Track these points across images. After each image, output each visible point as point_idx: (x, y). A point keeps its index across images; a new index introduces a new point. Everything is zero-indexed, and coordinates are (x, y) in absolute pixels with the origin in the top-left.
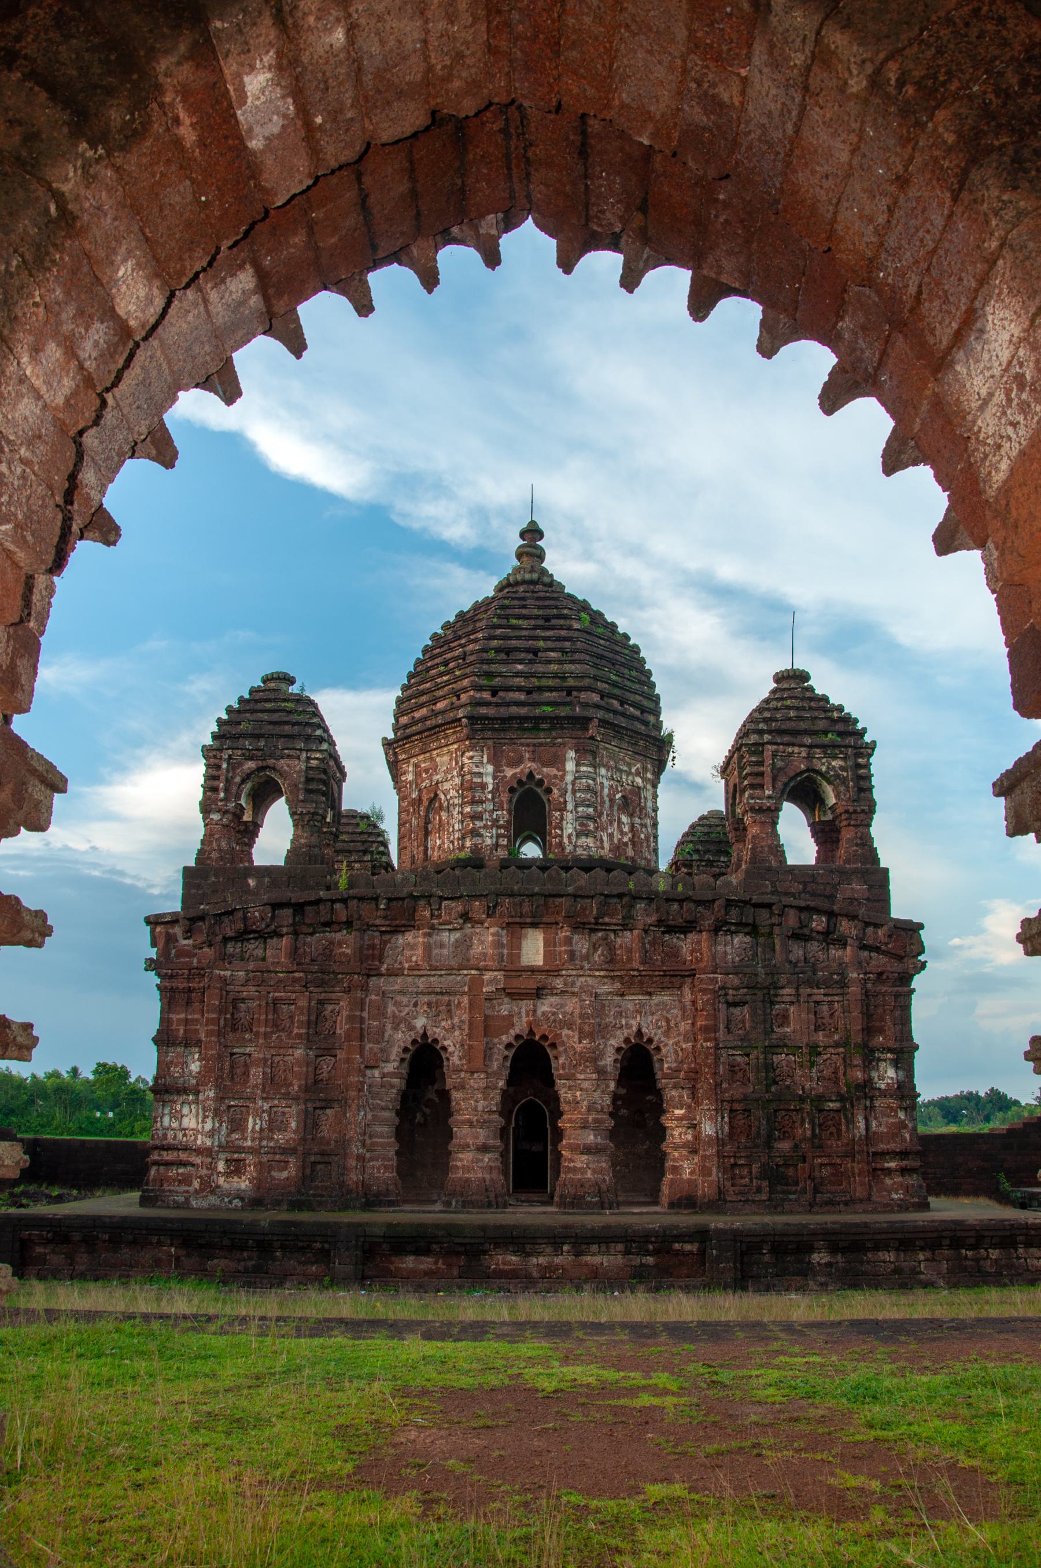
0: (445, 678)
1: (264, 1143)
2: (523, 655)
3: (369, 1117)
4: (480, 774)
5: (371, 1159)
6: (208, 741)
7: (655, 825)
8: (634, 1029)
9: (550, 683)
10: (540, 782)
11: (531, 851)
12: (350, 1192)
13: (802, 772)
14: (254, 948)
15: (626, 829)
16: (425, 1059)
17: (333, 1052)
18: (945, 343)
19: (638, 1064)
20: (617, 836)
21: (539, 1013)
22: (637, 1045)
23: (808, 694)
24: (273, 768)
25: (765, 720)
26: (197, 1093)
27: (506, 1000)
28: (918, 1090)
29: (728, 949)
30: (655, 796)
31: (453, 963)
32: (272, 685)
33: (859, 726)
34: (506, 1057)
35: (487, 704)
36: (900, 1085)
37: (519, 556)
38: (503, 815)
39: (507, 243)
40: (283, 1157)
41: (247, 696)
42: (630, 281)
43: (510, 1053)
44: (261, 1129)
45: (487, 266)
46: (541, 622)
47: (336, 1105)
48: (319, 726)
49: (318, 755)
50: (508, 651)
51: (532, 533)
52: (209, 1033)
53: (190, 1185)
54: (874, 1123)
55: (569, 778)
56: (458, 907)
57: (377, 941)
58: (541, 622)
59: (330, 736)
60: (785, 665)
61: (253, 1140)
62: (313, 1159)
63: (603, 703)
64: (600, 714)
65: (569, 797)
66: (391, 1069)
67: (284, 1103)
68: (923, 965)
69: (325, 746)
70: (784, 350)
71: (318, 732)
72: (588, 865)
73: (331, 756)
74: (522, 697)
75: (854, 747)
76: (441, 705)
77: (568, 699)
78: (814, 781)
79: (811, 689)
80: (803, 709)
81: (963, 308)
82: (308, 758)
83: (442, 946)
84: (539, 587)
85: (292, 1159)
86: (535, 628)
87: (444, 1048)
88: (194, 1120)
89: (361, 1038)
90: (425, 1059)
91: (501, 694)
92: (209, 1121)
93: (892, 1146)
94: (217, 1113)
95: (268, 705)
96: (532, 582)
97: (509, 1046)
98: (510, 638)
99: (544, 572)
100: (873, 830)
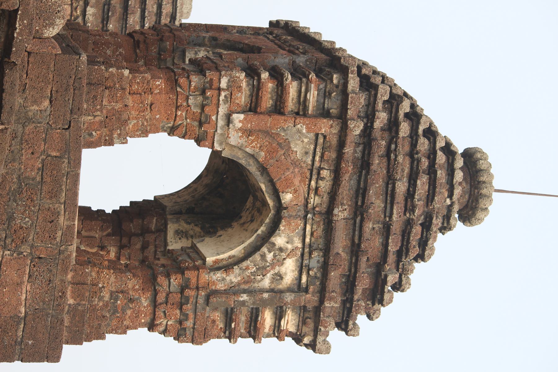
23: (437, 222)
25: (393, 126)
33: (361, 319)
75: (318, 310)
79: (445, 228)
80: (409, 207)
100: (140, 335)
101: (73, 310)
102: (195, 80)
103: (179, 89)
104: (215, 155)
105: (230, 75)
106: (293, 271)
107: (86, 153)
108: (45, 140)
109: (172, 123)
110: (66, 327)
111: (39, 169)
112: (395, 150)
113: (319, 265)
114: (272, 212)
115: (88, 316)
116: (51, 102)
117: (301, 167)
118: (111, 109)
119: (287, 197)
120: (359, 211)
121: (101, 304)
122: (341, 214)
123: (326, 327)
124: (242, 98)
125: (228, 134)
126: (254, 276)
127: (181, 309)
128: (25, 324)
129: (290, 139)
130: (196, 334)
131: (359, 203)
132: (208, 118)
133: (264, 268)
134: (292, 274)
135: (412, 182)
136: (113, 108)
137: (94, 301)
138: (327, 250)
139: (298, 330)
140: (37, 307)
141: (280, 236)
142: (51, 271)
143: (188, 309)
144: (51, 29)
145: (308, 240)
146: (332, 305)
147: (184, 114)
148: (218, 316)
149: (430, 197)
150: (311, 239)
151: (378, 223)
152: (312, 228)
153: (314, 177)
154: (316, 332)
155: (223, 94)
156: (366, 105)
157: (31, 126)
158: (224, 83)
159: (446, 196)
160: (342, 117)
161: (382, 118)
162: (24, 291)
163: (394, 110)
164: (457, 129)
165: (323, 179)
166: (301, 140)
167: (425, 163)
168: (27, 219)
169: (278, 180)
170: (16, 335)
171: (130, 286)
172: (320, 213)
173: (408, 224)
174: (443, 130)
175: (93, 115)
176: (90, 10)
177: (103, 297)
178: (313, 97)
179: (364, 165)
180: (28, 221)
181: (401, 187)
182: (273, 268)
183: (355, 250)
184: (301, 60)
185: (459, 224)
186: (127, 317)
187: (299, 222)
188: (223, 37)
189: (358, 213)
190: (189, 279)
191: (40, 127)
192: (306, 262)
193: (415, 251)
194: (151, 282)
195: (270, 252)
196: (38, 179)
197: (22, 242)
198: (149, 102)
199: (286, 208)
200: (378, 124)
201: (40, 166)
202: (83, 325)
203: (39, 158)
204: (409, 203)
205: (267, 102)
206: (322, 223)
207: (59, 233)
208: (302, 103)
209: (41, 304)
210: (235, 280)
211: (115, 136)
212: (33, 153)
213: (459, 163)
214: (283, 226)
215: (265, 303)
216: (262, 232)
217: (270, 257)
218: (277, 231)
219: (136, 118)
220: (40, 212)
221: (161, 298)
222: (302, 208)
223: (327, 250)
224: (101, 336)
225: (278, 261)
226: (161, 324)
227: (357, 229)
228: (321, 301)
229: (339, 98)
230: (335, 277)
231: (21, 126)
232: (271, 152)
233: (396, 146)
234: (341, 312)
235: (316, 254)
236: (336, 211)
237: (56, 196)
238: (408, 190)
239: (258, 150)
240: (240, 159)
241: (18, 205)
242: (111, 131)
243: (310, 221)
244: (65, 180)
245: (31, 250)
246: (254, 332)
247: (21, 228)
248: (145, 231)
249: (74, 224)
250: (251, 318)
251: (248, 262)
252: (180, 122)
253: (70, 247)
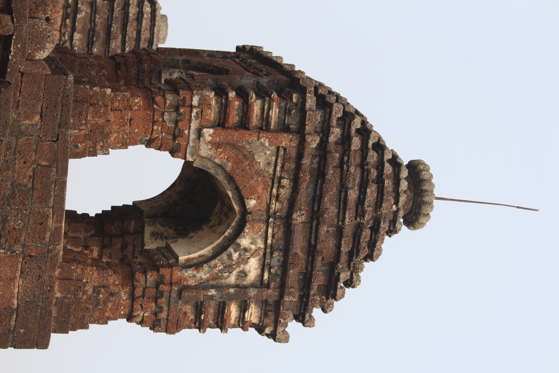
13: (242, 201)
23: (385, 226)
25: (346, 140)
33: (317, 312)
75: (278, 303)
78: (223, 222)
79: (392, 231)
80: (360, 212)
100: (120, 326)
101: (60, 303)
102: (170, 98)
103: (155, 106)
104: (187, 166)
105: (201, 94)
106: (256, 269)
107: (73, 163)
108: (36, 151)
109: (149, 136)
110: (54, 317)
111: (30, 177)
112: (348, 162)
113: (280, 264)
114: (238, 216)
115: (73, 308)
116: (41, 117)
117: (264, 176)
118: (94, 124)
119: (252, 203)
120: (315, 216)
121: (85, 297)
122: (299, 218)
123: (285, 319)
124: (212, 114)
125: (199, 147)
126: (222, 273)
127: (156, 302)
128: (17, 315)
129: (254, 151)
130: (169, 325)
131: (316, 209)
132: (181, 132)
133: (231, 266)
134: (255, 271)
135: (363, 190)
136: (97, 123)
137: (79, 294)
138: (286, 250)
139: (260, 321)
140: (28, 300)
141: (245, 238)
142: (40, 268)
143: (163, 301)
144: (42, 52)
145: (269, 241)
146: (291, 299)
147: (160, 128)
148: (189, 309)
149: (378, 204)
150: (272, 241)
151: (332, 226)
152: (273, 231)
153: (276, 185)
154: (276, 323)
155: (195, 111)
156: (322, 122)
157: (24, 139)
158: (195, 101)
159: (393, 203)
160: (301, 133)
161: (336, 133)
162: (17, 285)
163: (347, 126)
165: (283, 187)
166: (264, 152)
167: (374, 173)
168: (19, 221)
169: (244, 188)
170: (10, 325)
171: (111, 281)
172: (280, 217)
173: (359, 228)
174: (390, 144)
175: (79, 129)
176: (77, 36)
177: (87, 291)
178: (274, 113)
179: (320, 175)
180: (21, 223)
181: (353, 195)
182: (238, 266)
183: (312, 250)
184: (264, 81)
185: (404, 228)
186: (108, 309)
187: (262, 225)
188: (195, 60)
189: (314, 217)
190: (163, 275)
191: (32, 139)
192: (267, 261)
193: (365, 252)
194: (129, 279)
195: (236, 252)
196: (30, 185)
197: (15, 242)
198: (129, 117)
199: (250, 213)
200: (332, 139)
201: (31, 174)
202: (69, 316)
203: (30, 167)
204: (360, 209)
205: (234, 118)
206: (282, 227)
207: (48, 234)
208: (265, 119)
209: (32, 297)
210: (204, 277)
211: (98, 147)
212: (25, 163)
213: (405, 173)
214: (247, 229)
215: (231, 298)
216: (229, 234)
217: (235, 256)
218: (242, 233)
219: (117, 132)
220: (31, 215)
221: (138, 292)
222: (265, 213)
223: (286, 250)
224: (86, 327)
225: (243, 260)
226: (138, 315)
227: (313, 231)
228: (281, 296)
229: (298, 115)
230: (293, 273)
231: (14, 138)
232: (237, 163)
233: (349, 158)
234: (299, 305)
235: (277, 254)
236: (295, 216)
237: (45, 201)
238: (359, 197)
239: (225, 161)
240: (209, 168)
241: (11, 208)
242: (95, 144)
243: (272, 224)
244: (53, 186)
245: (23, 249)
246: (221, 323)
247: (14, 229)
249: (62, 226)
250: (218, 310)
251: (217, 261)
252: (156, 136)
253: (57, 247)
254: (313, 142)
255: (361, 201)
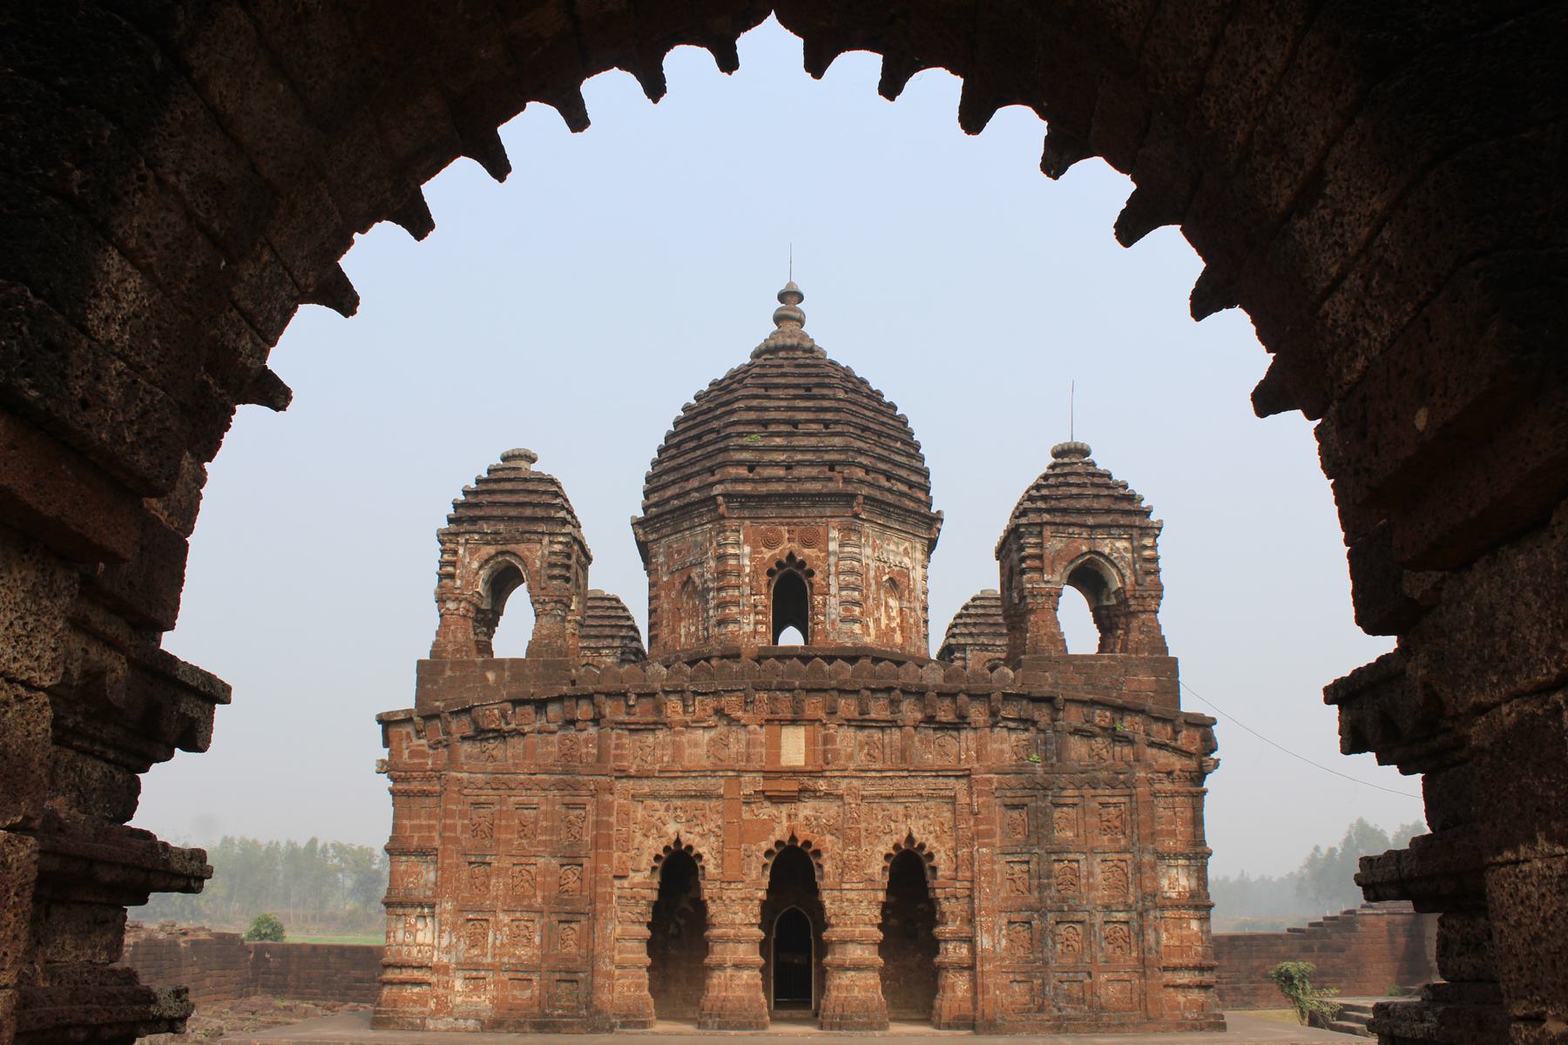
0: (698, 453)
1: (506, 960)
2: (783, 428)
3: (619, 930)
4: (736, 556)
5: (621, 977)
6: (445, 525)
7: (925, 609)
8: (905, 835)
9: (809, 457)
10: (803, 563)
11: (791, 637)
12: (599, 1012)
13: (1083, 554)
14: (493, 746)
15: (894, 614)
16: (679, 868)
17: (578, 861)
18: (1282, 205)
19: (909, 868)
20: (884, 621)
21: (801, 816)
22: (907, 851)
23: (1091, 469)
24: (514, 554)
25: (1043, 498)
26: (432, 906)
27: (767, 804)
28: (1212, 899)
29: (1006, 747)
30: (925, 578)
31: (706, 763)
32: (513, 464)
33: (1144, 504)
34: (765, 866)
35: (744, 480)
36: (1193, 895)
37: (778, 319)
38: (764, 600)
39: (746, 43)
40: (525, 975)
41: (485, 475)
42: (891, 87)
43: (770, 861)
44: (503, 945)
45: (723, 70)
46: (802, 392)
47: (582, 918)
48: (563, 508)
49: (561, 539)
50: (765, 423)
51: (790, 296)
52: (444, 840)
53: (425, 1004)
54: (1164, 936)
55: (832, 560)
56: (711, 702)
57: (626, 741)
58: (802, 392)
59: (574, 517)
60: (1063, 439)
61: (494, 956)
62: (558, 976)
63: (869, 478)
64: (865, 491)
65: (832, 580)
66: (643, 880)
67: (526, 916)
68: (1217, 763)
69: (568, 529)
70: (1072, 168)
71: (562, 514)
72: (853, 656)
73: (575, 539)
74: (781, 473)
75: (1141, 528)
76: (695, 483)
77: (830, 474)
78: (1097, 564)
79: (1093, 464)
80: (1084, 485)
81: (1308, 168)
82: (551, 542)
83: (696, 745)
84: (799, 354)
85: (535, 977)
86: (795, 397)
87: (699, 856)
88: (429, 935)
89: (609, 845)
90: (679, 868)
91: (758, 470)
92: (446, 936)
93: (1185, 961)
94: (454, 928)
95: (508, 486)
96: (792, 348)
97: (768, 853)
98: (766, 409)
99: (804, 336)
101: (1151, 653)
119: (1084, 549)
120: (1088, 511)
122: (1090, 521)
124: (1036, 576)
138: (1110, 526)
148: (1148, 579)
160: (1041, 525)
161: (1040, 504)
164: (1042, 463)
166: (1054, 544)
173: (1093, 485)
174: (1044, 470)
178: (1032, 540)
179: (1065, 511)
181: (1074, 491)
183: (1108, 511)
184: (1015, 547)
194: (1134, 614)
205: (1037, 563)
223: (1110, 526)
232: (1062, 559)
246: (1155, 560)
248: (1108, 617)
254: (1046, 517)
255: (1078, 485)
